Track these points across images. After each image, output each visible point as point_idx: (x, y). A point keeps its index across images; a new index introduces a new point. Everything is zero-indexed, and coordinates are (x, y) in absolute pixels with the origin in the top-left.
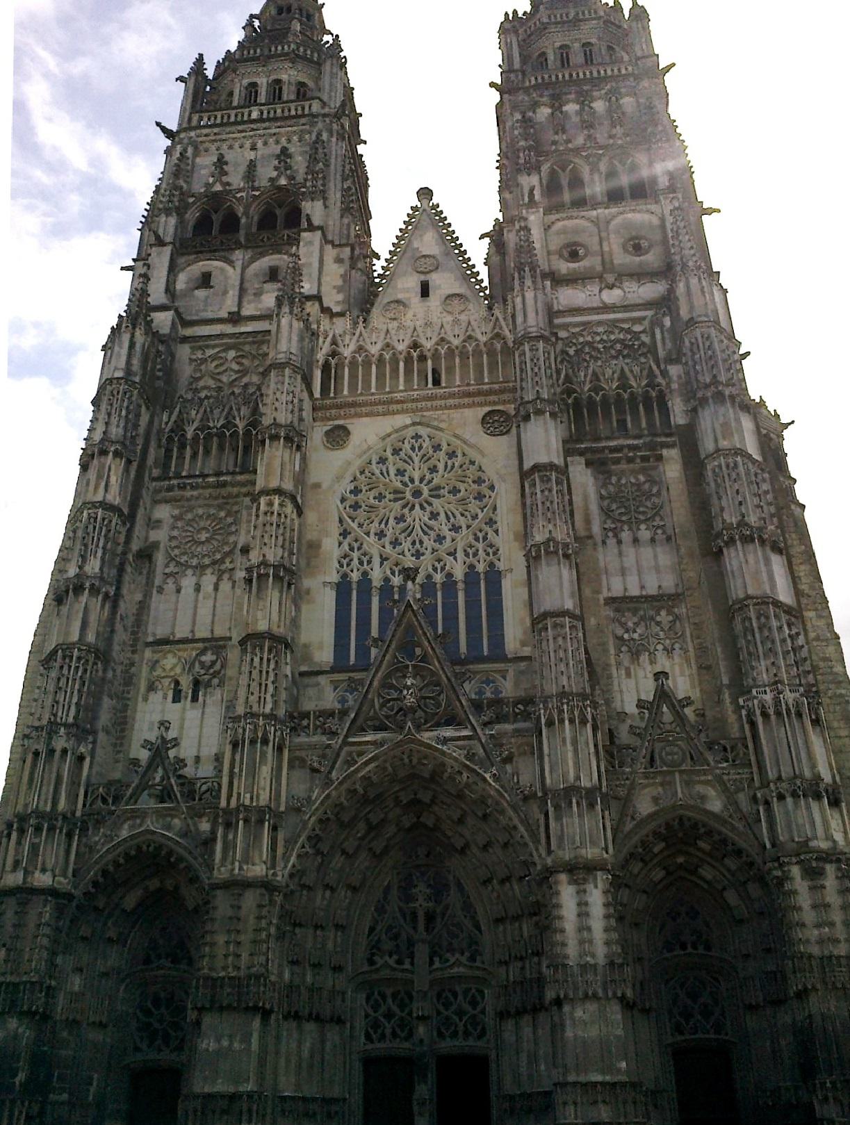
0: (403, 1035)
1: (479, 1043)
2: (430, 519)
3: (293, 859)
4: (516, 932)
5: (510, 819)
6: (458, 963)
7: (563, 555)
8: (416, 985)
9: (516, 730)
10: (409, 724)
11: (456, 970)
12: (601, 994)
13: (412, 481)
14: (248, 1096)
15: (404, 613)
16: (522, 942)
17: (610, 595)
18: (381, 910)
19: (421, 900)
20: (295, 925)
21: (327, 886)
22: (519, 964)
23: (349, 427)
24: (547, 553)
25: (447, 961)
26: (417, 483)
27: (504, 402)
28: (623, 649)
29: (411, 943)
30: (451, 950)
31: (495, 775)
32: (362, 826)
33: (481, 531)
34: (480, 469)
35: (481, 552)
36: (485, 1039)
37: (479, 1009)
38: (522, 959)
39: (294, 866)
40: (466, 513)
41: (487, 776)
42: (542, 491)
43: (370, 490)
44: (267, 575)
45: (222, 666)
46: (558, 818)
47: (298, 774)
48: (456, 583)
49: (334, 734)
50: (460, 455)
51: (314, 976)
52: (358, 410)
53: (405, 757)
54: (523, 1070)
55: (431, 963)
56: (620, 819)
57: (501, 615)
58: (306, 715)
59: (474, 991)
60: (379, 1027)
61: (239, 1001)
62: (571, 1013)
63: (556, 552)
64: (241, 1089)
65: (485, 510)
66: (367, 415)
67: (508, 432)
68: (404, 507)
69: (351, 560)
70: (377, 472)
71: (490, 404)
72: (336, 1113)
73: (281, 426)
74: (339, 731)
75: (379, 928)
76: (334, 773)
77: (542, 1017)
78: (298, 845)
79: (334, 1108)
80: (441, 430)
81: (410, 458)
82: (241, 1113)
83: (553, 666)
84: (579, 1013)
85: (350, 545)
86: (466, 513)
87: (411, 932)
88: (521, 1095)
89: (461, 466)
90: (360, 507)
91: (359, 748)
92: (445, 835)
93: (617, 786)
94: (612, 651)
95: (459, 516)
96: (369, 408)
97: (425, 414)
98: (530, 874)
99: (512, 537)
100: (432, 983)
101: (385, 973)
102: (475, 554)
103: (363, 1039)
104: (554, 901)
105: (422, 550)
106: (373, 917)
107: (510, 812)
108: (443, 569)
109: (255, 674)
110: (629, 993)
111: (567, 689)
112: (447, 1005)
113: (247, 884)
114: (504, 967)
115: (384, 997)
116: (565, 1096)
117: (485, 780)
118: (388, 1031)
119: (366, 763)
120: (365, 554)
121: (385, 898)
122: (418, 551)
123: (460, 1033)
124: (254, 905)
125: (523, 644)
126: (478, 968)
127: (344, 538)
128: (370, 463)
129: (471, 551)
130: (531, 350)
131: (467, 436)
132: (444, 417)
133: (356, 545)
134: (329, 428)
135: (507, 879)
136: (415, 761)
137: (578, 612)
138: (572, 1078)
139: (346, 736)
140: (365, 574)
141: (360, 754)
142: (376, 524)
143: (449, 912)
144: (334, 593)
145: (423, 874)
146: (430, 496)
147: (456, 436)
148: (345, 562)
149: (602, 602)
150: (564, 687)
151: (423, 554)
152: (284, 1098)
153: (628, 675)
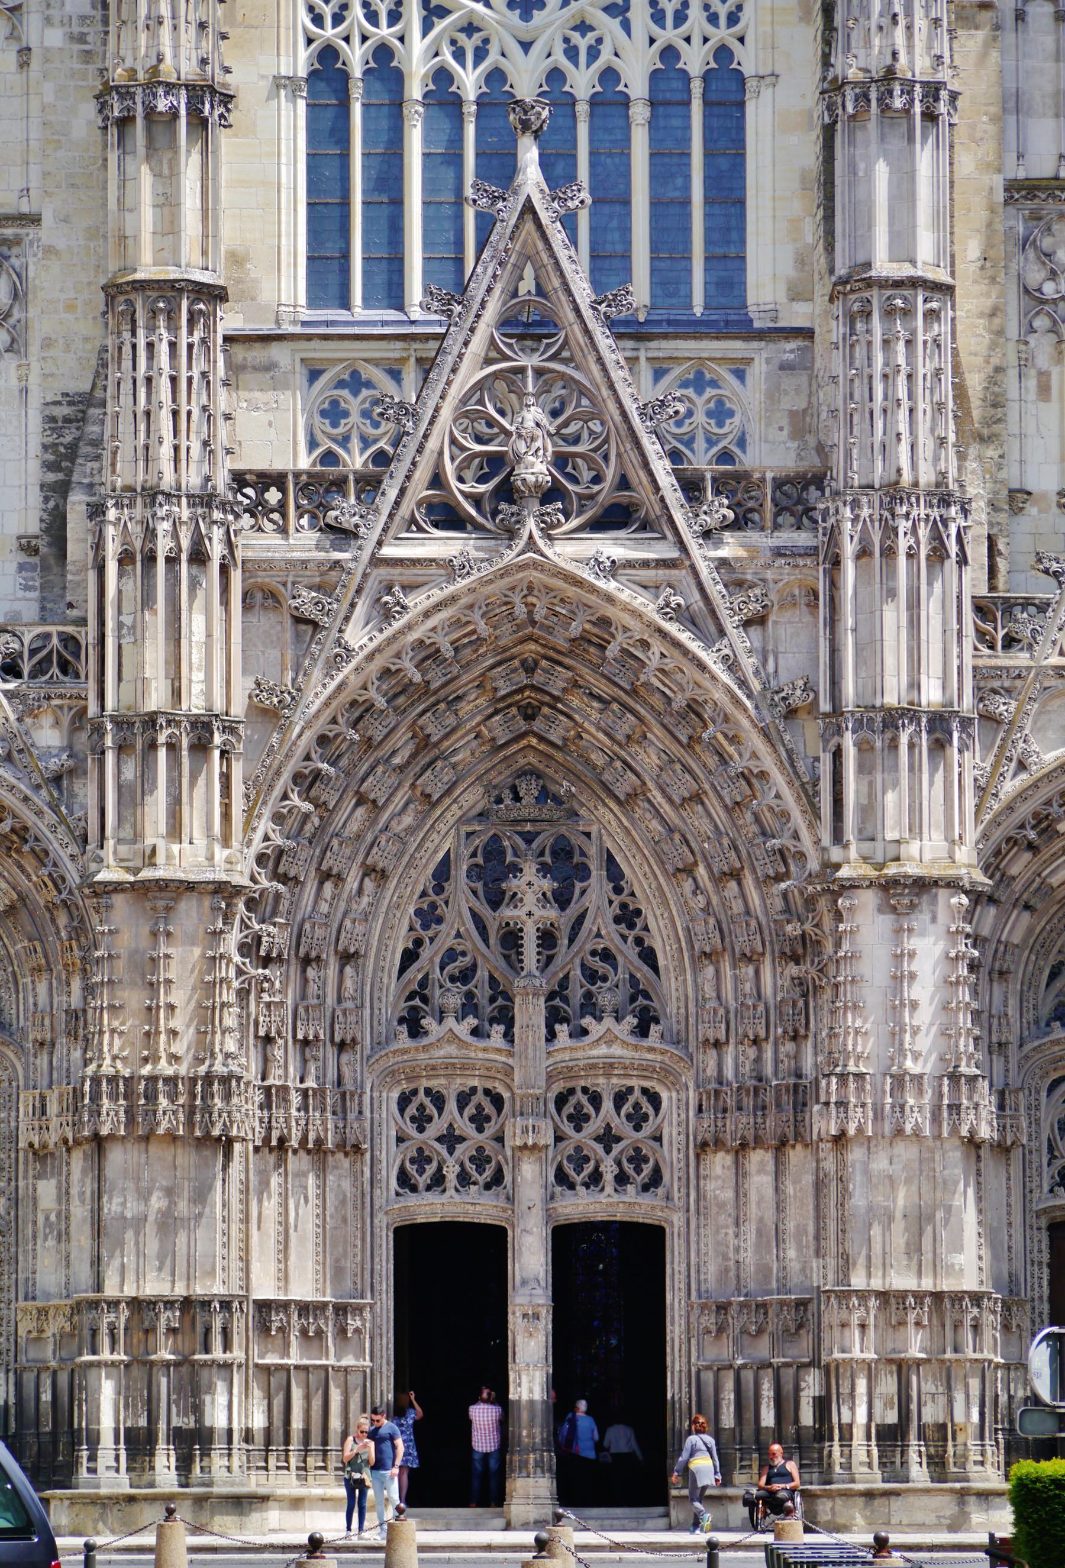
0: (481, 1179)
1: (646, 1200)
3: (264, 825)
4: (748, 987)
5: (754, 755)
6: (609, 1039)
7: (923, 114)
8: (516, 1078)
9: (778, 552)
10: (531, 525)
11: (602, 1050)
12: (927, 1132)
14: (221, 1303)
15: (516, 226)
16: (761, 1008)
17: (1021, 174)
18: (429, 917)
19: (530, 900)
20: (266, 962)
21: (325, 876)
22: (752, 1052)
24: (885, 108)
25: (585, 1032)
28: (1037, 323)
29: (500, 992)
30: (590, 1006)
31: (726, 658)
32: (402, 746)
36: (661, 1191)
37: (648, 1129)
38: (756, 1042)
39: (266, 838)
41: (708, 658)
44: (173, 114)
45: (16, 296)
46: (862, 768)
47: (265, 621)
48: (625, 102)
49: (342, 535)
51: (305, 1061)
53: (517, 599)
54: (749, 1257)
55: (551, 1036)
56: (995, 766)
57: (741, 203)
58: (278, 480)
59: (637, 1093)
60: (429, 1161)
61: (190, 1123)
62: (866, 1165)
63: (907, 111)
64: (199, 1290)
72: (357, 1331)
74: (362, 530)
75: (426, 953)
76: (349, 629)
77: (796, 1155)
78: (277, 792)
79: (353, 1323)
82: (208, 1331)
83: (878, 413)
84: (880, 1163)
87: (502, 963)
88: (743, 1305)
91: (409, 574)
92: (587, 761)
93: (994, 691)
94: (1013, 331)
98: (786, 875)
100: (550, 1077)
101: (452, 1050)
103: (394, 1183)
104: (846, 946)
106: (411, 929)
107: (757, 742)
108: (593, 53)
109: (164, 384)
110: (985, 1132)
111: (907, 478)
112: (579, 1120)
113: (190, 887)
114: (713, 1053)
115: (439, 1101)
116: (844, 1314)
117: (702, 667)
118: (451, 1173)
119: (427, 614)
121: (439, 889)
123: (609, 1177)
124: (201, 930)
125: (797, 294)
126: (652, 1050)
135: (735, 875)
136: (539, 614)
137: (942, 276)
138: (858, 1281)
139: (380, 544)
140: (383, 53)
141: (407, 588)
143: (587, 924)
144: (302, 104)
145: (529, 838)
149: (1000, 196)
150: (899, 471)
152: (264, 1307)
153: (1044, 390)
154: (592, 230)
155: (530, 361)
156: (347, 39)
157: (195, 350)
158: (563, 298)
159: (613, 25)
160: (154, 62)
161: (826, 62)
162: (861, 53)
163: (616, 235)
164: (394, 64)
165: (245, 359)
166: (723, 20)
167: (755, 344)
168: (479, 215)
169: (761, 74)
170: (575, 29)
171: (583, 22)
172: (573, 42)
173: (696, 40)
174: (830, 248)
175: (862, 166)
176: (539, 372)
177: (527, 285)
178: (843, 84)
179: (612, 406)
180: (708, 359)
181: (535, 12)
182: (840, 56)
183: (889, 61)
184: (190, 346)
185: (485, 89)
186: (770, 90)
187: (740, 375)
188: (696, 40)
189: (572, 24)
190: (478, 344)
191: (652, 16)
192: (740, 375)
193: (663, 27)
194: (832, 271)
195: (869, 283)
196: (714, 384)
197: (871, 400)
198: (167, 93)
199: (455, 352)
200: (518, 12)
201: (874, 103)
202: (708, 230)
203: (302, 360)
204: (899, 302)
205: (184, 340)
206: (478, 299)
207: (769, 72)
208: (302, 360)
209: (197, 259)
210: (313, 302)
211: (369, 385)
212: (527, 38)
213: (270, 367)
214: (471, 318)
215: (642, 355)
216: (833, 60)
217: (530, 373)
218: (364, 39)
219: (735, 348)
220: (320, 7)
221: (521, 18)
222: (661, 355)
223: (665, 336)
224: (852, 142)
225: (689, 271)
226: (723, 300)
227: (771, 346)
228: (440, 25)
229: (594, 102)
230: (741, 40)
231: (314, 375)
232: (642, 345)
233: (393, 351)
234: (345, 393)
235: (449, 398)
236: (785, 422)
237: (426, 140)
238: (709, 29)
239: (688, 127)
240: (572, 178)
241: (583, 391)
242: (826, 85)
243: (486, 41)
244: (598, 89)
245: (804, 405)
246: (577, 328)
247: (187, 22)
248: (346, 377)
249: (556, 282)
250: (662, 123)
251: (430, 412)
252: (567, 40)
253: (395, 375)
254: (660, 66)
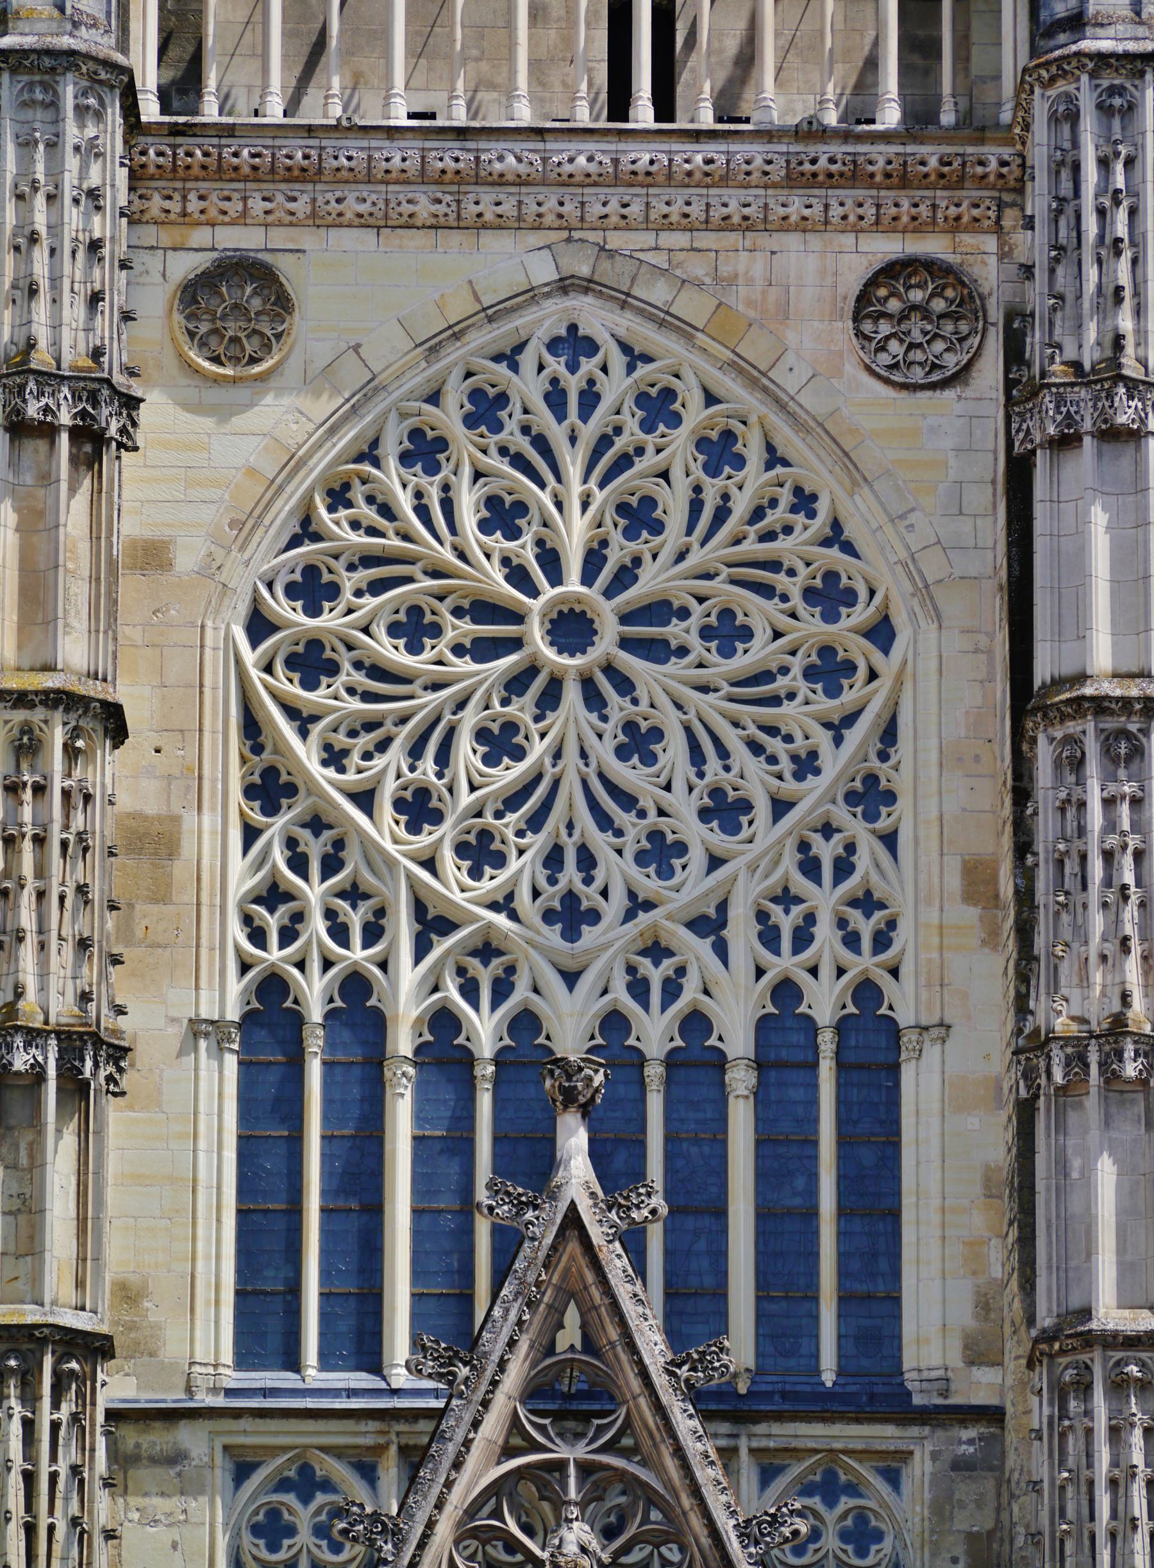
2: (622, 753)
13: (551, 561)
15: (554, 1247)
23: (284, 266)
24: (1111, 1077)
26: (573, 585)
27: (955, 226)
33: (827, 830)
34: (835, 536)
35: (825, 932)
40: (774, 745)
42: (1109, 803)
43: (377, 587)
44: (38, 1075)
48: (719, 1062)
50: (754, 455)
52: (326, 195)
57: (895, 1215)
65: (854, 736)
66: (362, 222)
67: (961, 376)
68: (516, 684)
69: (298, 917)
70: (405, 502)
71: (893, 226)
73: (49, 379)
80: (683, 329)
81: (542, 444)
85: (291, 843)
86: (774, 745)
89: (757, 514)
90: (333, 669)
95: (740, 753)
96: (375, 194)
97: (615, 240)
99: (954, 882)
102: (803, 938)
105: (589, 896)
108: (672, 989)
120: (353, 894)
122: (571, 898)
127: (271, 810)
128: (370, 454)
129: (786, 922)
130: (1106, 110)
131: (789, 381)
132: (698, 268)
133: (315, 848)
134: (203, 261)
142: (396, 755)
144: (231, 1062)
146: (626, 643)
147: (739, 367)
148: (272, 922)
151: (594, 917)
154: (669, 1253)
155: (572, 1453)
156: (301, 965)
157: (62, 1433)
158: (624, 1357)
159: (703, 947)
160: (10, 997)
161: (1022, 1008)
162: (1075, 994)
163: (705, 1263)
164: (372, 1002)
165: (138, 1446)
166: (866, 943)
167: (914, 1431)
168: (498, 1231)
169: (924, 1023)
170: (643, 953)
171: (656, 943)
172: (642, 971)
173: (826, 971)
174: (1028, 1285)
175: (1076, 1163)
176: (586, 1469)
177: (569, 1336)
178: (1048, 1040)
179: (696, 1522)
180: (846, 1452)
181: (585, 928)
182: (1043, 998)
183: (1116, 1007)
184: (55, 1426)
185: (507, 1041)
186: (937, 1048)
187: (893, 1478)
188: (826, 971)
189: (640, 945)
190: (493, 1426)
191: (760, 935)
192: (893, 1478)
193: (777, 953)
194: (1031, 1320)
195: (1089, 1340)
196: (852, 1490)
197: (1092, 1518)
198: (28, 1045)
199: (459, 1436)
200: (558, 927)
201: (1094, 1070)
202: (842, 1257)
203: (226, 1448)
204: (1133, 1369)
205: (46, 1416)
206: (495, 1357)
207: (935, 1020)
208: (226, 1448)
209: (68, 1293)
210: (243, 1361)
211: (327, 1486)
212: (571, 965)
213: (176, 1458)
214: (484, 1387)
215: (743, 1445)
216: (1032, 1004)
217: (572, 1470)
218: (327, 964)
219: (885, 1435)
220: (262, 918)
221: (563, 936)
222: (772, 1444)
223: (779, 1417)
224: (1061, 1126)
225: (816, 1318)
226: (865, 1362)
227: (940, 1433)
228: (442, 946)
229: (672, 1061)
230: (894, 972)
231: (242, 1471)
232: (743, 1430)
233: (365, 1435)
234: (290, 1499)
235: (448, 1509)
236: (960, 1551)
237: (419, 1117)
238: (846, 956)
239: (814, 1102)
240: (639, 1174)
241: (652, 1499)
242: (1021, 1042)
243: (511, 970)
244: (679, 1042)
245: (989, 1525)
246: (643, 1402)
247: (60, 938)
248: (292, 1473)
249: (613, 1333)
250: (774, 1094)
251: (419, 1530)
252: (631, 969)
253: (368, 1472)
254: (771, 1009)
